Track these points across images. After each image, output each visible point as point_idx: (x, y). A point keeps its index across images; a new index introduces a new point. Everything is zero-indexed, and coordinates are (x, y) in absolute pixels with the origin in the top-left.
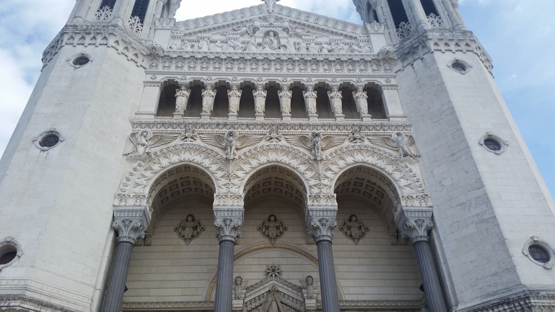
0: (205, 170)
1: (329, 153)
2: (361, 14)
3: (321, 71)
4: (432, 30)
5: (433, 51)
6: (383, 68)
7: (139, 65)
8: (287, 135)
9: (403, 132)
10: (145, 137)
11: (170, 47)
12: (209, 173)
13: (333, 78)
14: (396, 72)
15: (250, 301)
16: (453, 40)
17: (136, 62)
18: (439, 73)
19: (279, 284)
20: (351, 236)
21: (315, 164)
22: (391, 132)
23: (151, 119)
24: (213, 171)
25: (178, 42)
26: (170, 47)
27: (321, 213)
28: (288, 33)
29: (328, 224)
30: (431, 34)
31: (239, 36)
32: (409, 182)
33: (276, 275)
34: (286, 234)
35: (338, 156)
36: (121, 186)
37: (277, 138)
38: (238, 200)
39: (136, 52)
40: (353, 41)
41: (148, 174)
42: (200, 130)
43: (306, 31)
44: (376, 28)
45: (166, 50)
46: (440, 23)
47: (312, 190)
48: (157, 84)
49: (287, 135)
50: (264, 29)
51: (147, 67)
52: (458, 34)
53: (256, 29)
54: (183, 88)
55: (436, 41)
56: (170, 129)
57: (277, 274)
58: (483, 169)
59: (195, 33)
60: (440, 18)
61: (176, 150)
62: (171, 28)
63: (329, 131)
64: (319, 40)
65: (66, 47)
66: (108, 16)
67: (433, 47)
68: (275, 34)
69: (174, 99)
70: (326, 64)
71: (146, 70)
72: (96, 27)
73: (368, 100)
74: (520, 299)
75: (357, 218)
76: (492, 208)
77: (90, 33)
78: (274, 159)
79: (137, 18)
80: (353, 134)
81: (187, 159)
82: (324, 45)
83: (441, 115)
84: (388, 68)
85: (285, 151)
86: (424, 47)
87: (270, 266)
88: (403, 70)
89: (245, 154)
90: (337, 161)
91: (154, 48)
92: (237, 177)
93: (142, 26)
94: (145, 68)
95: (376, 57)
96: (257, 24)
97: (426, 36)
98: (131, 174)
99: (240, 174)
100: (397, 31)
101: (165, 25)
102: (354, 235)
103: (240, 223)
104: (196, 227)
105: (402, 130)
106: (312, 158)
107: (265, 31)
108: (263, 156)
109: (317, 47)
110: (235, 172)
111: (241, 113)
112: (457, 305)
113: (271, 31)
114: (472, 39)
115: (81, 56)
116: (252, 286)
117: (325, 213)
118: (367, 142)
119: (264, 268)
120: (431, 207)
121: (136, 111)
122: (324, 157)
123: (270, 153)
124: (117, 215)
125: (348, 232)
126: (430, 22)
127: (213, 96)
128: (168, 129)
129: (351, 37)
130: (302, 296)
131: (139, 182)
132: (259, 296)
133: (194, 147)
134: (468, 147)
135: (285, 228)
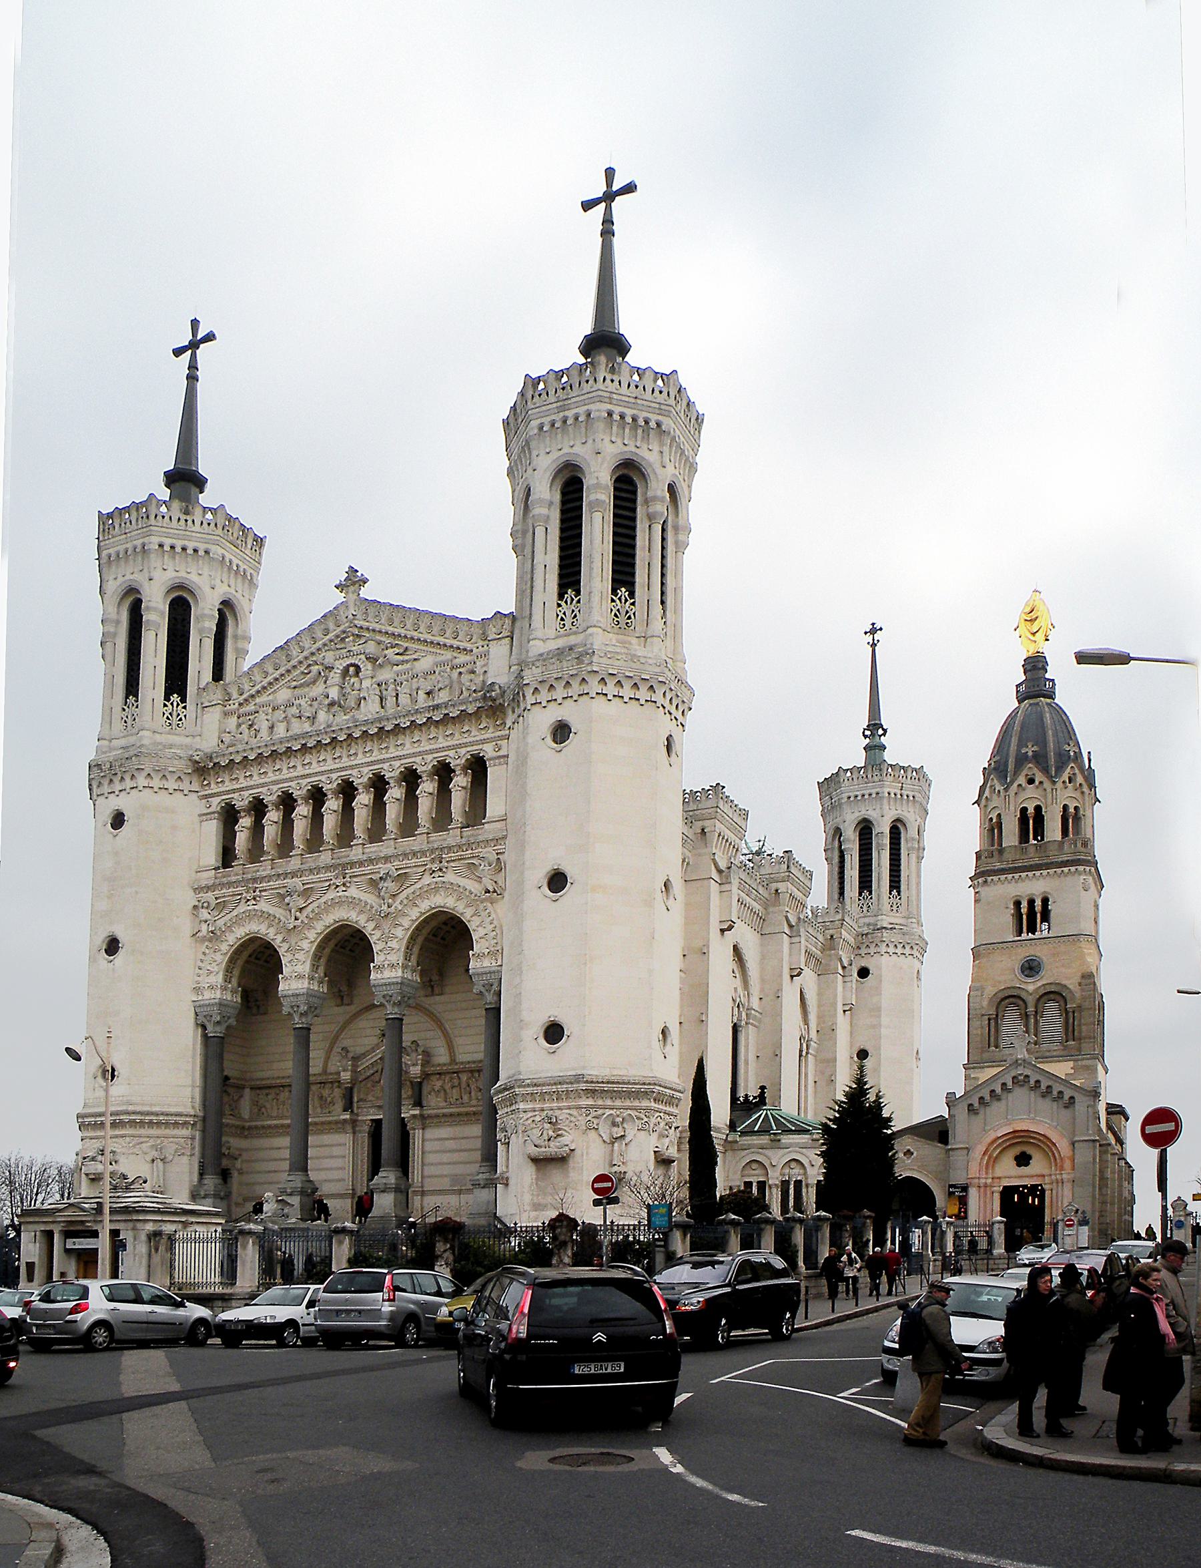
1: (399, 901)
9: (495, 848)
10: (207, 908)
22: (480, 850)
25: (233, 720)
31: (307, 689)
35: (411, 903)
40: (462, 658)
43: (401, 651)
47: (379, 957)
50: (341, 664)
54: (243, 814)
59: (253, 696)
61: (238, 921)
68: (358, 669)
96: (329, 657)
107: (341, 668)
110: (299, 944)
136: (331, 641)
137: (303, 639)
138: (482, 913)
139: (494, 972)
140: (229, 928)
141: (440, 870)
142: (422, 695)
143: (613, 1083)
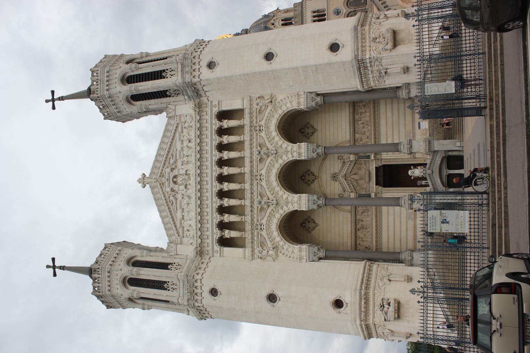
0: (282, 216)
1: (271, 145)
2: (143, 116)
3: (208, 148)
4: (183, 77)
5: (200, 79)
6: (205, 109)
7: (209, 261)
8: (257, 170)
11: (191, 244)
12: (285, 214)
13: (213, 141)
14: (208, 101)
15: (350, 189)
16: (191, 66)
17: (208, 262)
18: (218, 78)
19: (341, 174)
20: (313, 133)
21: (278, 154)
22: (254, 108)
23: (248, 251)
24: (283, 212)
25: (185, 240)
26: (191, 244)
27: (309, 152)
28: (174, 169)
29: (315, 148)
30: (187, 79)
32: (289, 102)
33: (337, 176)
34: (312, 170)
35: (272, 140)
36: (294, 260)
37: (260, 176)
38: (302, 196)
39: (201, 263)
41: (286, 247)
42: (255, 221)
43: (172, 157)
44: (171, 111)
45: (195, 246)
46: (172, 70)
47: (295, 156)
48: (222, 249)
49: (257, 170)
51: (209, 256)
52: (187, 63)
53: (173, 190)
54: (223, 234)
55: (192, 77)
56: (255, 238)
57: (336, 175)
58: (286, 65)
59: (176, 230)
60: (167, 70)
61: (269, 234)
62: (175, 245)
63: (254, 145)
64: (179, 148)
65: (203, 303)
66: (173, 284)
67: (196, 80)
68: (175, 177)
69: (231, 238)
70: (202, 144)
71: (211, 257)
72: (188, 287)
73: (229, 119)
74: (359, 64)
75: (301, 129)
76: (310, 65)
77: (193, 290)
78: (275, 177)
79: (169, 267)
80: (257, 130)
81: (275, 227)
82: (185, 144)
83: (247, 81)
84: (205, 106)
85: (269, 171)
86: (195, 84)
87: (331, 179)
88: (208, 97)
89: (272, 194)
90: (275, 141)
91: (197, 253)
92: (287, 198)
93: (174, 263)
94: (210, 257)
95: (197, 113)
96: (168, 189)
97: (189, 82)
98: (287, 256)
99: (285, 196)
100: (173, 96)
101: (173, 249)
102: (312, 131)
103: (316, 196)
104: (308, 221)
105: (253, 102)
106: (274, 155)
107: (173, 184)
108: (273, 184)
109: (185, 149)
111: (242, 198)
112: (358, 88)
113: (173, 180)
114: (190, 54)
115: (210, 293)
116: (343, 188)
117: (309, 150)
118: (262, 123)
119: (333, 182)
120: (304, 92)
121: (243, 259)
122: (274, 149)
123: (271, 180)
124: (311, 260)
125: (310, 134)
126: (171, 77)
127: (229, 215)
128: (255, 239)
129: (177, 127)
130: (348, 162)
131: (291, 251)
132: (348, 185)
133: (268, 223)
134: (272, 71)
135: (308, 170)
136: (162, 190)
137: (159, 203)
138: (280, 105)
139: (307, 96)
140: (272, 240)
141: (260, 127)
142: (190, 145)
143: (359, 21)
